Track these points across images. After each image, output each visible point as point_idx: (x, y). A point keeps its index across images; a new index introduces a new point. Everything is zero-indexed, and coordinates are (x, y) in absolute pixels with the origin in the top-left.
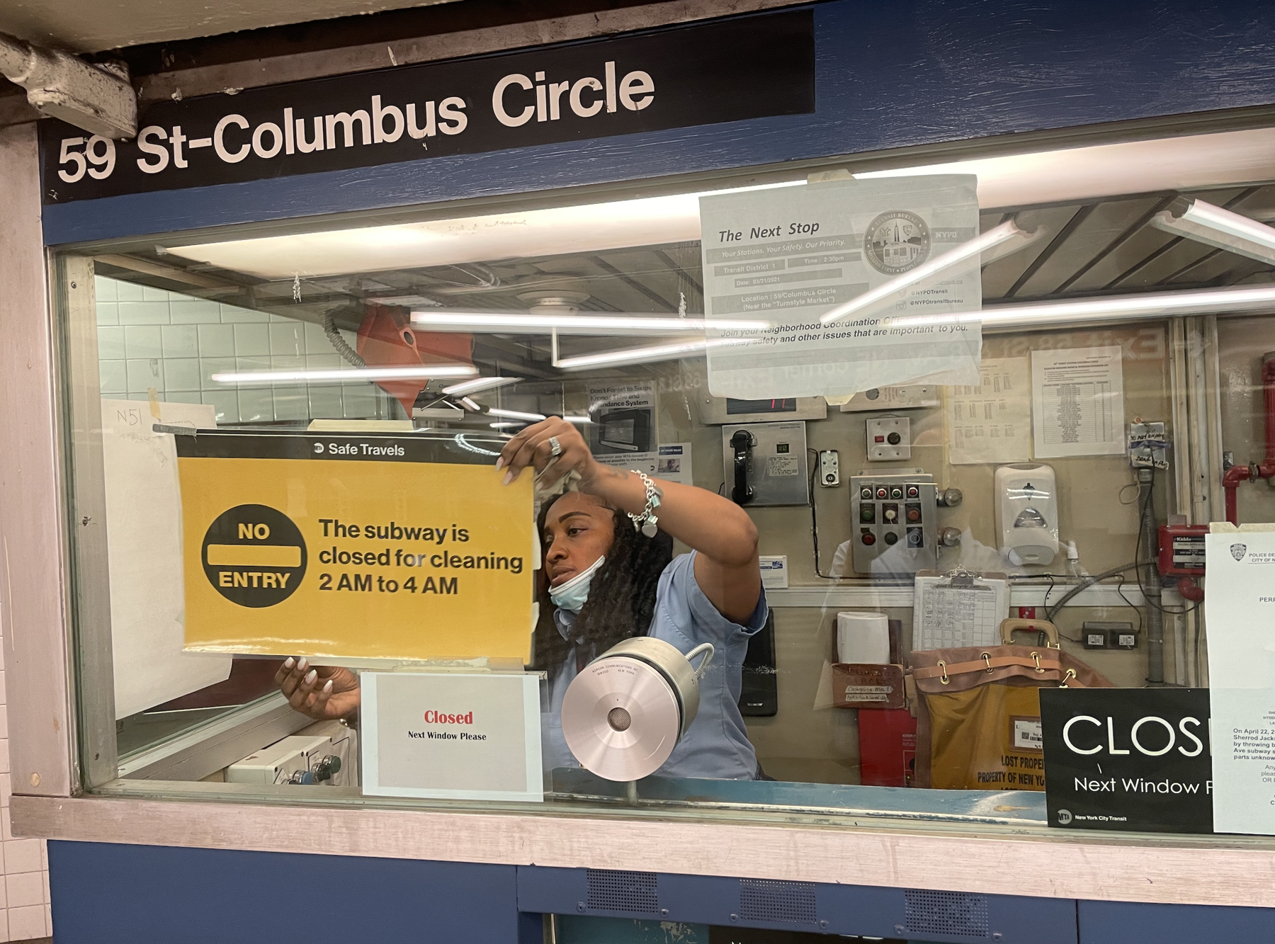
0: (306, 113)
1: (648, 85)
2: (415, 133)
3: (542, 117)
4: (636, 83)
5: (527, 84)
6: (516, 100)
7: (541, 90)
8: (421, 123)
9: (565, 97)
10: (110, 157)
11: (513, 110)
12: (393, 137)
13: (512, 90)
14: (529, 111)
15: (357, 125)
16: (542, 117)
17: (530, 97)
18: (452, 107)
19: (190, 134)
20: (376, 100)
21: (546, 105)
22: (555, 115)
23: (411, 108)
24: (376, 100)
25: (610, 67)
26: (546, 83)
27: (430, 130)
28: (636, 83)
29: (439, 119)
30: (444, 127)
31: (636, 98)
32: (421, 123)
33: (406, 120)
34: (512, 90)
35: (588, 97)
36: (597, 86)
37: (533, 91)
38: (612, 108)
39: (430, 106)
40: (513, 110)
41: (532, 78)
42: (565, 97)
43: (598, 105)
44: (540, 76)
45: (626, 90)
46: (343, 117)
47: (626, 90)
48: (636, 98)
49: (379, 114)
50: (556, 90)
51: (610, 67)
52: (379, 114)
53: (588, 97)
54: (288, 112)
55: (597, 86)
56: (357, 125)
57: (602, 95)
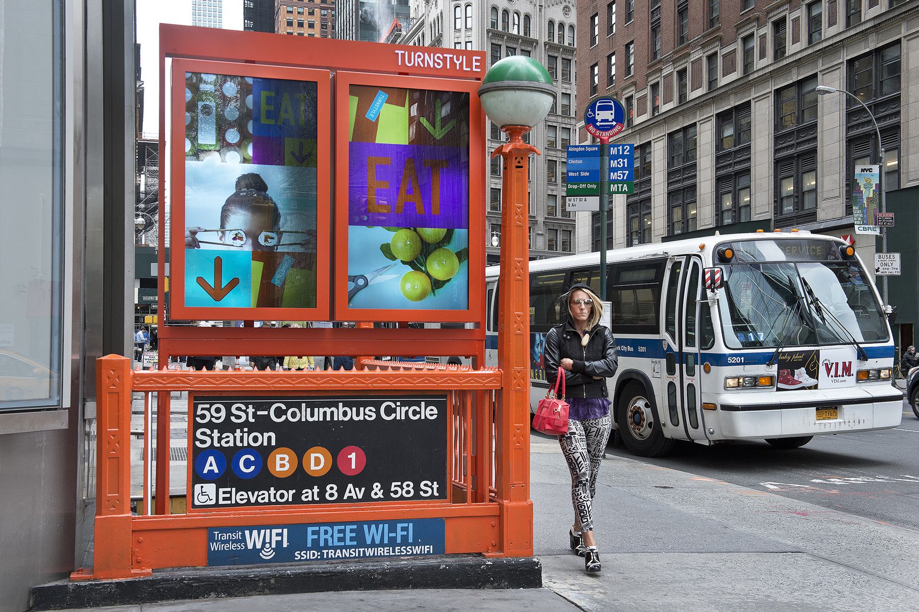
0: (311, 406)
1: (436, 411)
2: (355, 418)
3: (398, 418)
4: (432, 410)
5: (393, 406)
6: (389, 411)
7: (398, 409)
8: (358, 415)
9: (407, 412)
10: (223, 414)
11: (388, 414)
12: (346, 419)
13: (388, 407)
14: (393, 416)
15: (332, 413)
16: (398, 418)
17: (394, 411)
18: (370, 410)
19: (257, 407)
20: (341, 405)
21: (400, 413)
22: (403, 418)
23: (354, 409)
24: (341, 405)
25: (423, 404)
26: (400, 406)
27: (361, 418)
28: (432, 410)
29: (365, 414)
30: (366, 417)
31: (431, 415)
32: (358, 415)
33: (352, 414)
34: (388, 407)
35: (415, 413)
36: (418, 409)
37: (395, 409)
38: (423, 417)
39: (362, 409)
40: (388, 414)
41: (395, 402)
42: (407, 412)
43: (418, 416)
44: (398, 404)
45: (428, 412)
46: (326, 409)
47: (428, 412)
48: (431, 415)
49: (341, 409)
50: (404, 409)
51: (423, 404)
52: (341, 409)
53: (415, 413)
54: (304, 405)
55: (418, 409)
56: (332, 413)
57: (420, 413)
